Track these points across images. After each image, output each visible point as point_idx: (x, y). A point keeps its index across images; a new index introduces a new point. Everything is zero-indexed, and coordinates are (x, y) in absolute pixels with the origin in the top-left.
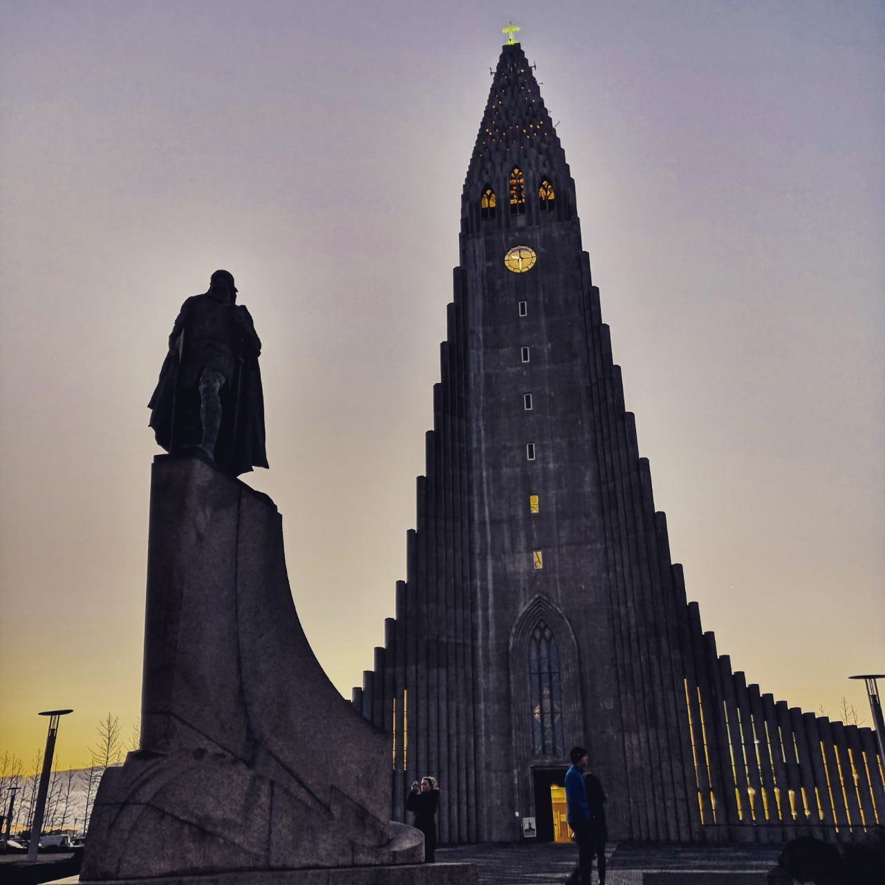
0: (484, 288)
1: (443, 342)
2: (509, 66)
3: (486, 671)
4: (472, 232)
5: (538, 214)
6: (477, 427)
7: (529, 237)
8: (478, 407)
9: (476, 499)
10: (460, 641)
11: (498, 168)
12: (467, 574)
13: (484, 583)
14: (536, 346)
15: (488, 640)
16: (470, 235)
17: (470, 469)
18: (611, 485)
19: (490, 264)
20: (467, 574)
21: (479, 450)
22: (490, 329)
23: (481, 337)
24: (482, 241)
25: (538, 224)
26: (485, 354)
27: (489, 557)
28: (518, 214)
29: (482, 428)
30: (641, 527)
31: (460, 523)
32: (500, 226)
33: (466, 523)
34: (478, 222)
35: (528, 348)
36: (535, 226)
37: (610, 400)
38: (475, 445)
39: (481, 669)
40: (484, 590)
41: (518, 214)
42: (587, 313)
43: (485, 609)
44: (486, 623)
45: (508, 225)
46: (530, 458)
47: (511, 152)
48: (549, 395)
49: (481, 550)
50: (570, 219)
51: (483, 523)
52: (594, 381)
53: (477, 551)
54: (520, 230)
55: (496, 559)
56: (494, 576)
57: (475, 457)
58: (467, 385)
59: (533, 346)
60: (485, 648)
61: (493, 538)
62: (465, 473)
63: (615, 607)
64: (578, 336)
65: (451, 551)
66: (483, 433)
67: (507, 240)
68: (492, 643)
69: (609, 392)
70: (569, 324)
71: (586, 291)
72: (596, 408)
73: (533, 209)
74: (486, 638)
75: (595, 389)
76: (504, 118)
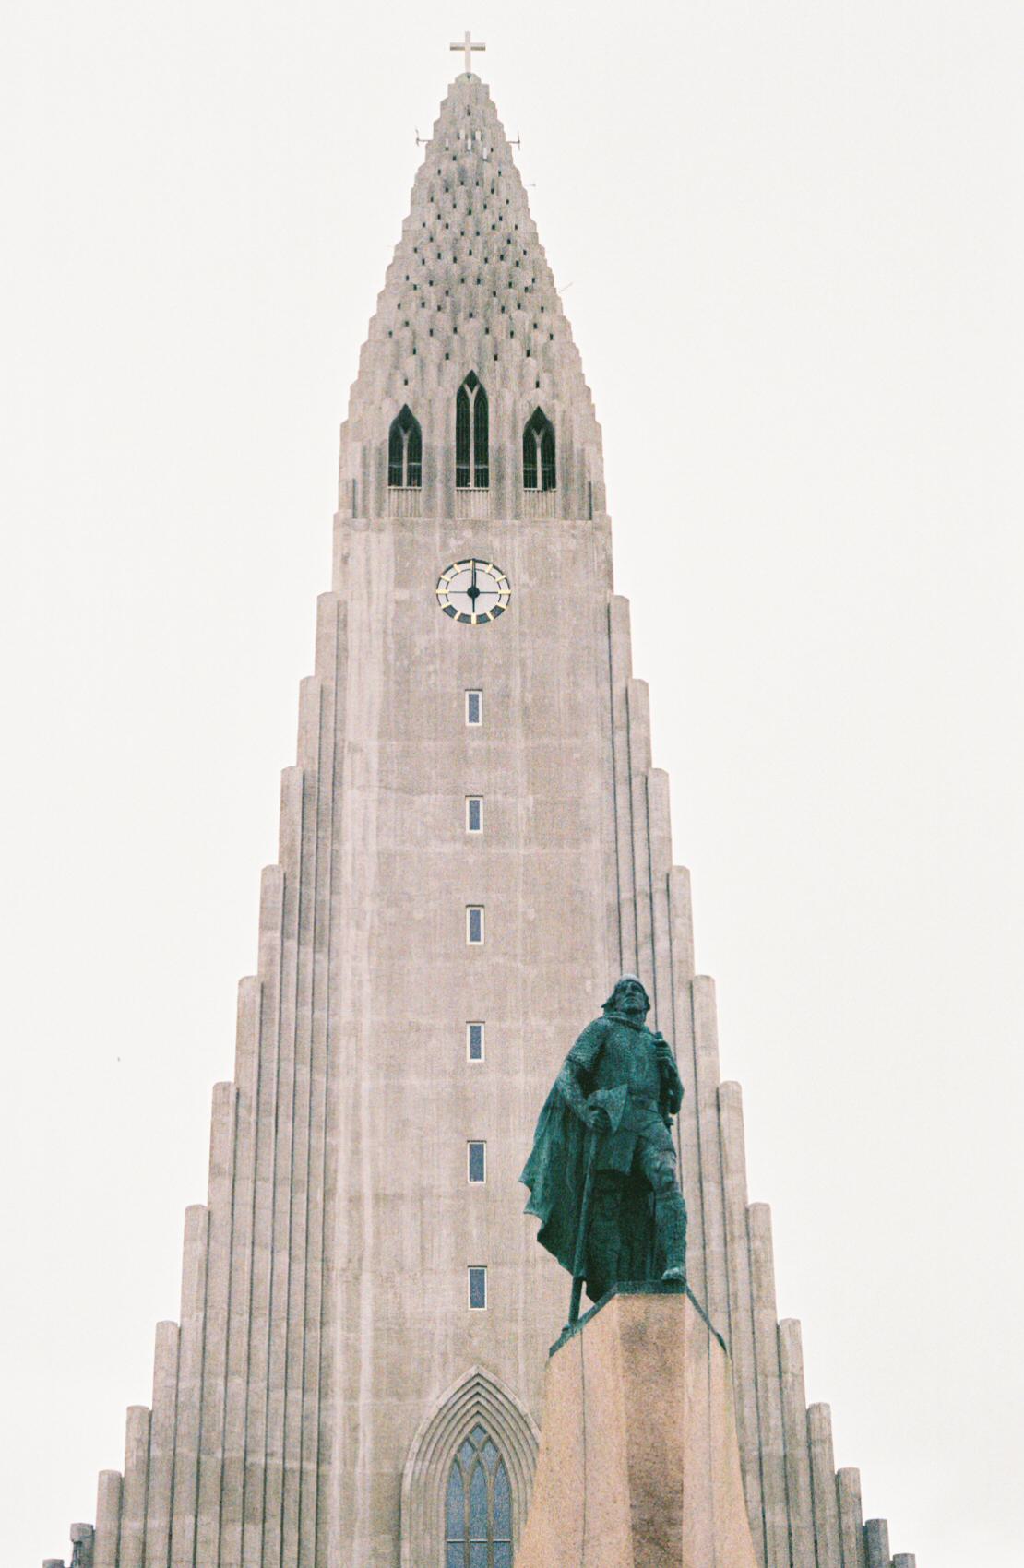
0: (385, 646)
2: (462, 137)
3: (348, 1533)
5: (517, 497)
7: (496, 544)
8: (358, 926)
9: (342, 1141)
10: (293, 1464)
11: (432, 371)
12: (315, 1313)
13: (352, 1335)
15: (354, 1464)
16: (361, 521)
17: (331, 1071)
19: (403, 595)
20: (315, 1313)
21: (355, 1030)
22: (394, 746)
23: (375, 766)
24: (387, 538)
25: (517, 516)
27: (366, 1277)
29: (366, 977)
31: (305, 1198)
32: (430, 509)
33: (320, 1197)
34: (379, 488)
35: (481, 800)
36: (509, 521)
37: (662, 945)
38: (345, 1015)
39: (334, 1529)
40: (352, 1350)
42: (620, 738)
43: (352, 1394)
45: (449, 514)
46: (472, 1057)
48: (524, 914)
50: (591, 518)
51: (355, 1200)
52: (626, 894)
53: (339, 1262)
54: (476, 525)
55: (384, 1281)
56: (377, 1318)
58: (334, 872)
59: (492, 797)
60: (348, 1487)
61: (377, 1234)
62: (320, 1078)
64: (595, 787)
65: (282, 1258)
66: (367, 989)
67: (444, 545)
68: (364, 1472)
69: (661, 925)
70: (577, 755)
72: (628, 955)
73: (508, 482)
74: (350, 1460)
76: (448, 257)
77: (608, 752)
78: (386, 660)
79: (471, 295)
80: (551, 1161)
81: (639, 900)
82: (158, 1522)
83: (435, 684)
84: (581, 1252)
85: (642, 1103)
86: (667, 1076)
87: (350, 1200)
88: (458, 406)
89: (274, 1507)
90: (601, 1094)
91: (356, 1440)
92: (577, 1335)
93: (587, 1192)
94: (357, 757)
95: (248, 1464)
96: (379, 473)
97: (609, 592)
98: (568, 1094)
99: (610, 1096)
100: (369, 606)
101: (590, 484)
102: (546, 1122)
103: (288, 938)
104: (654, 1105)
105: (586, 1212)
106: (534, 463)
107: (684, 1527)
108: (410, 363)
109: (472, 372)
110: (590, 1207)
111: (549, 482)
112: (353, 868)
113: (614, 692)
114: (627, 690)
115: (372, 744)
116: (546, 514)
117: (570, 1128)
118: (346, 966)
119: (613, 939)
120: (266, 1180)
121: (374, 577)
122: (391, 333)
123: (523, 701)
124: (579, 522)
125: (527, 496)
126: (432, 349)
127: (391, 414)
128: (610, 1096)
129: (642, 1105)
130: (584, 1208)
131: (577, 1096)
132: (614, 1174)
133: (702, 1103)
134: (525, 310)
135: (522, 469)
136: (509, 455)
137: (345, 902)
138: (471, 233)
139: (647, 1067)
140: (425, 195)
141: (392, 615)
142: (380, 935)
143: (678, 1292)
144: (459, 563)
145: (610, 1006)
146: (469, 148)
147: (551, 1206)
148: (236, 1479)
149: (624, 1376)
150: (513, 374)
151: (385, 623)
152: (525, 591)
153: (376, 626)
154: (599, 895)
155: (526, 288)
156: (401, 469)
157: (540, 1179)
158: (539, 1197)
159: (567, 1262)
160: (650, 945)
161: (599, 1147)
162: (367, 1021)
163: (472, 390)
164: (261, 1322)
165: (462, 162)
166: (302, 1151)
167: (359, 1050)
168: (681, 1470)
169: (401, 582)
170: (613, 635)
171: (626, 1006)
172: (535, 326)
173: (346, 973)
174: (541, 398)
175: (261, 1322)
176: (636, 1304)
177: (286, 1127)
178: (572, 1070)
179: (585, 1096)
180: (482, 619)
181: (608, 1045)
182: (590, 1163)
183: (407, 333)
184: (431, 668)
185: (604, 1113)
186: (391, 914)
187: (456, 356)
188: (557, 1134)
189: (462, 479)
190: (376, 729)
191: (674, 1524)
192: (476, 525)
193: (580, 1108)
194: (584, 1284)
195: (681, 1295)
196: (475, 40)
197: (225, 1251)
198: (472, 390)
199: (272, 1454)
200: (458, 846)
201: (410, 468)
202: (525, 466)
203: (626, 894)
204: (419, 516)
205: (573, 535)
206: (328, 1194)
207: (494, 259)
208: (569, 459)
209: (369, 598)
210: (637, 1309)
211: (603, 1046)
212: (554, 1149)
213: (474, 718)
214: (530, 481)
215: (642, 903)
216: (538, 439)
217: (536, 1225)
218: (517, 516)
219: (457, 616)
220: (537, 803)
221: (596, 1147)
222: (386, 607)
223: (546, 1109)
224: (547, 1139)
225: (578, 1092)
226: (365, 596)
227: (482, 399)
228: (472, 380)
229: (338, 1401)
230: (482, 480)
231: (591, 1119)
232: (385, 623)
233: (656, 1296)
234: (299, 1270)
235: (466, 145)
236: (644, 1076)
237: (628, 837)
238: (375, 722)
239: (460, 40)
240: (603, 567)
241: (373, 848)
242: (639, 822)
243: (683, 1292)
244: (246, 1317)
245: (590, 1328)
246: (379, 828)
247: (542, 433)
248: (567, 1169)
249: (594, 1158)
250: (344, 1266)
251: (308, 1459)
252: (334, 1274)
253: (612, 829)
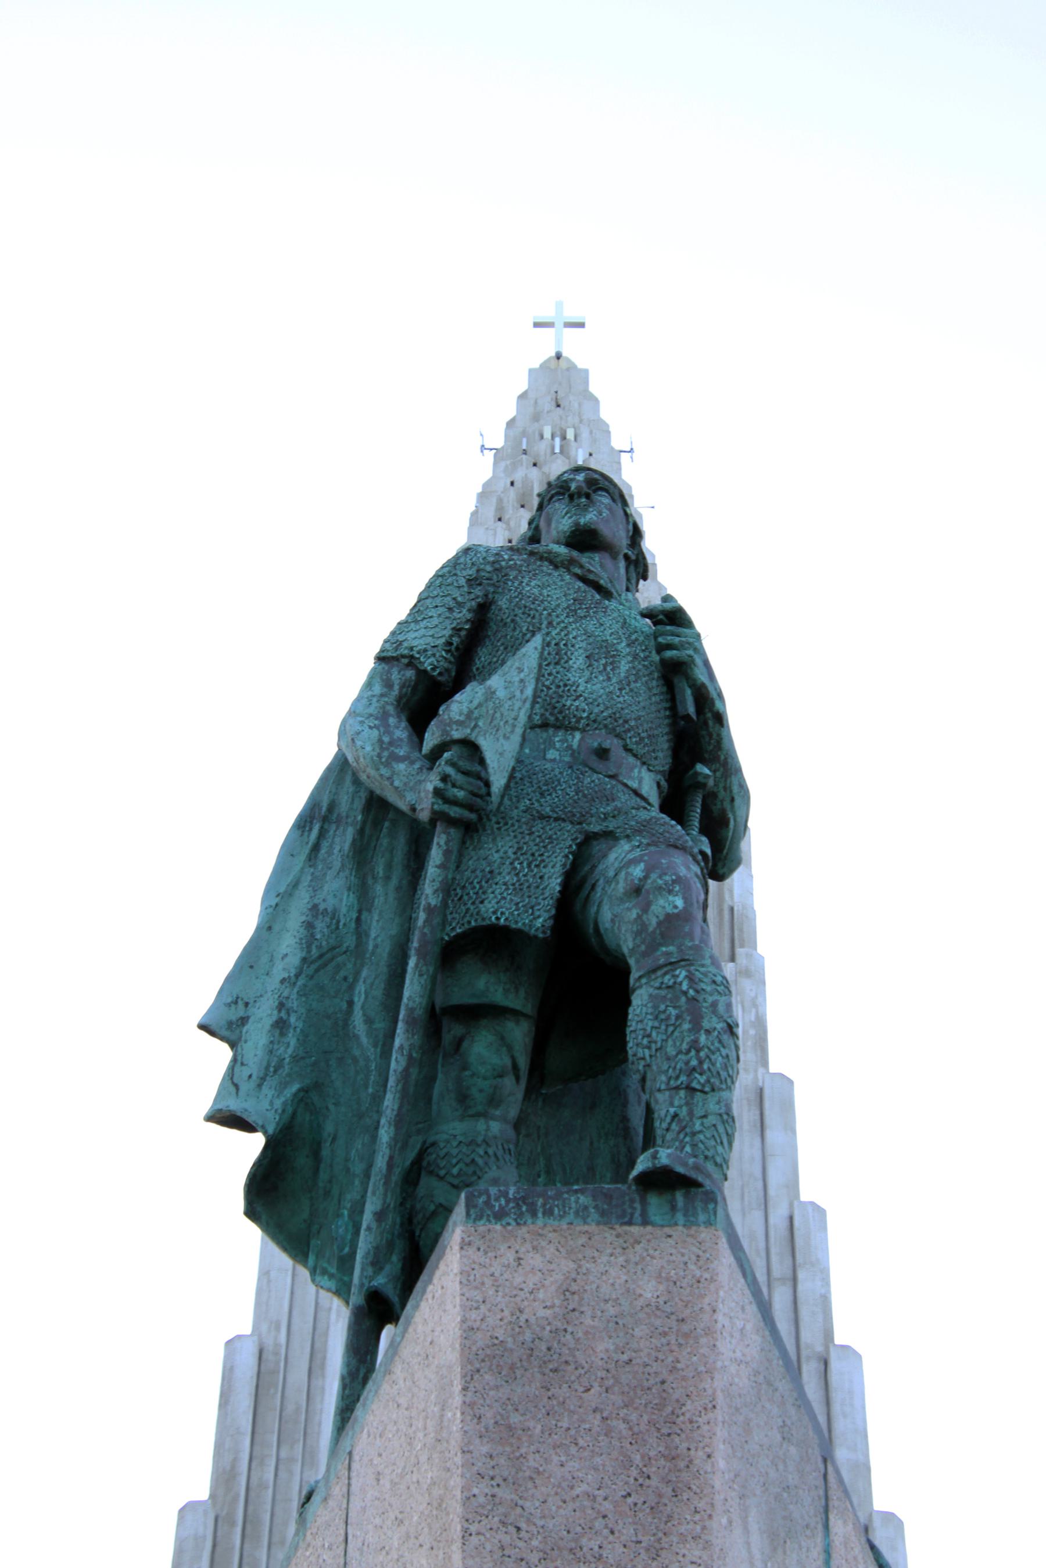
1: (239, 1337)
2: (547, 435)
80: (304, 960)
84: (379, 1216)
85: (602, 753)
93: (411, 1011)
97: (761, 1070)
99: (491, 694)
101: (732, 909)
102: (303, 857)
113: (772, 1221)
114: (791, 1219)
117: (380, 870)
139: (624, 666)
140: (490, 513)
146: (557, 450)
147: (295, 1087)
149: (466, 1534)
157: (264, 1014)
161: (456, 860)
165: (546, 469)
170: (769, 1134)
176: (535, 1260)
178: (388, 684)
181: (503, 603)
182: (422, 916)
195: (704, 1234)
210: (533, 1280)
211: (483, 613)
212: (320, 925)
221: (442, 866)
223: (303, 823)
224: (302, 901)
235: (553, 448)
240: (752, 1032)
243: (709, 1223)
248: (361, 988)
249: (434, 901)
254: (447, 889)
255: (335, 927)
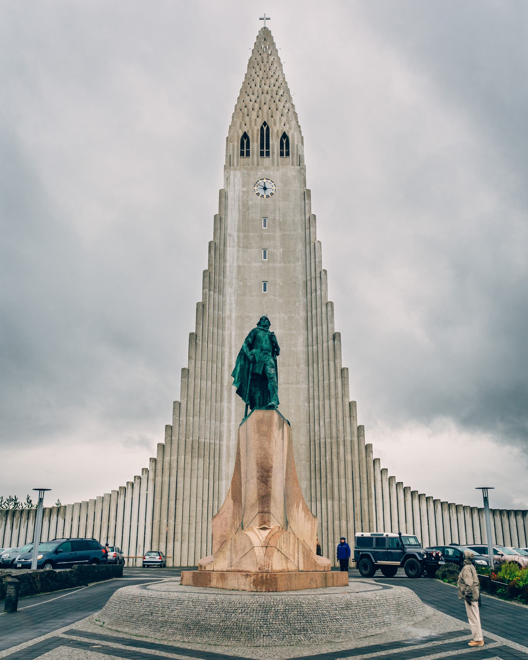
0: (239, 205)
2: (263, 48)
3: (228, 461)
4: (233, 165)
5: (278, 160)
6: (230, 300)
7: (272, 174)
13: (229, 405)
14: (272, 250)
15: (230, 441)
17: (223, 329)
18: (315, 347)
21: (230, 317)
22: (241, 234)
26: (238, 251)
28: (265, 156)
29: (233, 302)
30: (332, 376)
33: (220, 366)
35: (267, 250)
37: (319, 292)
38: (227, 313)
39: (224, 459)
41: (265, 156)
43: (229, 421)
44: (229, 431)
45: (258, 165)
47: (262, 111)
48: (279, 284)
49: (229, 383)
50: (300, 166)
52: (309, 278)
57: (227, 322)
59: (270, 250)
60: (228, 448)
62: (220, 331)
63: (312, 425)
64: (300, 247)
65: (209, 383)
66: (234, 305)
69: (318, 287)
70: (295, 237)
71: (307, 217)
72: (309, 296)
73: (275, 155)
75: (309, 283)
77: (304, 236)
78: (239, 209)
79: (265, 98)
81: (312, 279)
82: (174, 457)
83: (253, 216)
84: (248, 397)
86: (274, 345)
87: (229, 366)
88: (261, 132)
89: (207, 453)
90: (254, 351)
91: (230, 435)
92: (246, 422)
94: (231, 238)
95: (199, 441)
96: (238, 153)
97: (305, 188)
98: (245, 350)
100: (234, 193)
103: (211, 291)
104: (270, 354)
105: (250, 385)
106: (283, 149)
107: (272, 478)
108: (247, 119)
109: (265, 121)
110: (251, 384)
111: (288, 154)
112: (230, 270)
113: (306, 217)
114: (310, 217)
115: (235, 234)
116: (286, 164)
118: (227, 298)
119: (305, 291)
120: (205, 361)
121: (236, 184)
122: (241, 110)
123: (279, 220)
124: (296, 167)
125: (280, 159)
126: (254, 114)
127: (241, 134)
128: (256, 351)
129: (266, 354)
130: (249, 384)
131: (247, 351)
132: (257, 374)
133: (329, 339)
134: (281, 102)
135: (280, 151)
136: (275, 147)
137: (227, 281)
138: (265, 77)
141: (241, 195)
142: (237, 290)
143: (273, 409)
144: (260, 180)
145: (259, 324)
146: (265, 51)
147: (240, 383)
148: (196, 446)
150: (278, 121)
151: (239, 197)
152: (280, 188)
153: (236, 199)
154: (301, 278)
155: (281, 95)
156: (244, 152)
157: (237, 375)
158: (236, 380)
159: (244, 399)
160: (315, 293)
161: (253, 366)
162: (234, 315)
163: (265, 127)
164: (203, 401)
166: (215, 353)
167: (231, 323)
168: (272, 462)
169: (243, 186)
171: (263, 324)
172: (284, 107)
173: (228, 301)
174: (286, 129)
175: (203, 401)
177: (210, 346)
179: (250, 351)
180: (268, 196)
183: (246, 109)
184: (253, 211)
185: (254, 356)
186: (241, 283)
187: (260, 116)
188: (242, 362)
189: (262, 154)
190: (236, 229)
191: (270, 477)
192: (266, 168)
193: (249, 354)
194: (249, 406)
195: (273, 410)
196: (267, 16)
197: (193, 380)
198: (265, 127)
199: (206, 439)
200: (260, 264)
201: (246, 151)
202: (280, 150)
203: (309, 278)
204: (249, 166)
205: (295, 171)
206: (223, 364)
207: (272, 86)
208: (293, 147)
209: (235, 191)
213: (265, 226)
214: (282, 154)
215: (313, 280)
216: (284, 141)
217: (234, 388)
218: (278, 165)
219: (260, 196)
220: (283, 251)
222: (239, 193)
223: (239, 355)
225: (248, 350)
226: (233, 190)
227: (268, 129)
228: (265, 124)
229: (225, 423)
230: (268, 154)
231: (251, 358)
232: (239, 197)
233: (266, 411)
234: (214, 386)
235: (264, 51)
236: (266, 345)
237: (309, 261)
238: (236, 227)
239: (262, 17)
241: (235, 264)
242: (313, 257)
244: (199, 400)
245: (249, 419)
246: (237, 259)
247: (286, 139)
250: (227, 385)
251: (217, 440)
252: (224, 388)
253: (305, 258)
254: (253, 368)
255: (243, 367)
